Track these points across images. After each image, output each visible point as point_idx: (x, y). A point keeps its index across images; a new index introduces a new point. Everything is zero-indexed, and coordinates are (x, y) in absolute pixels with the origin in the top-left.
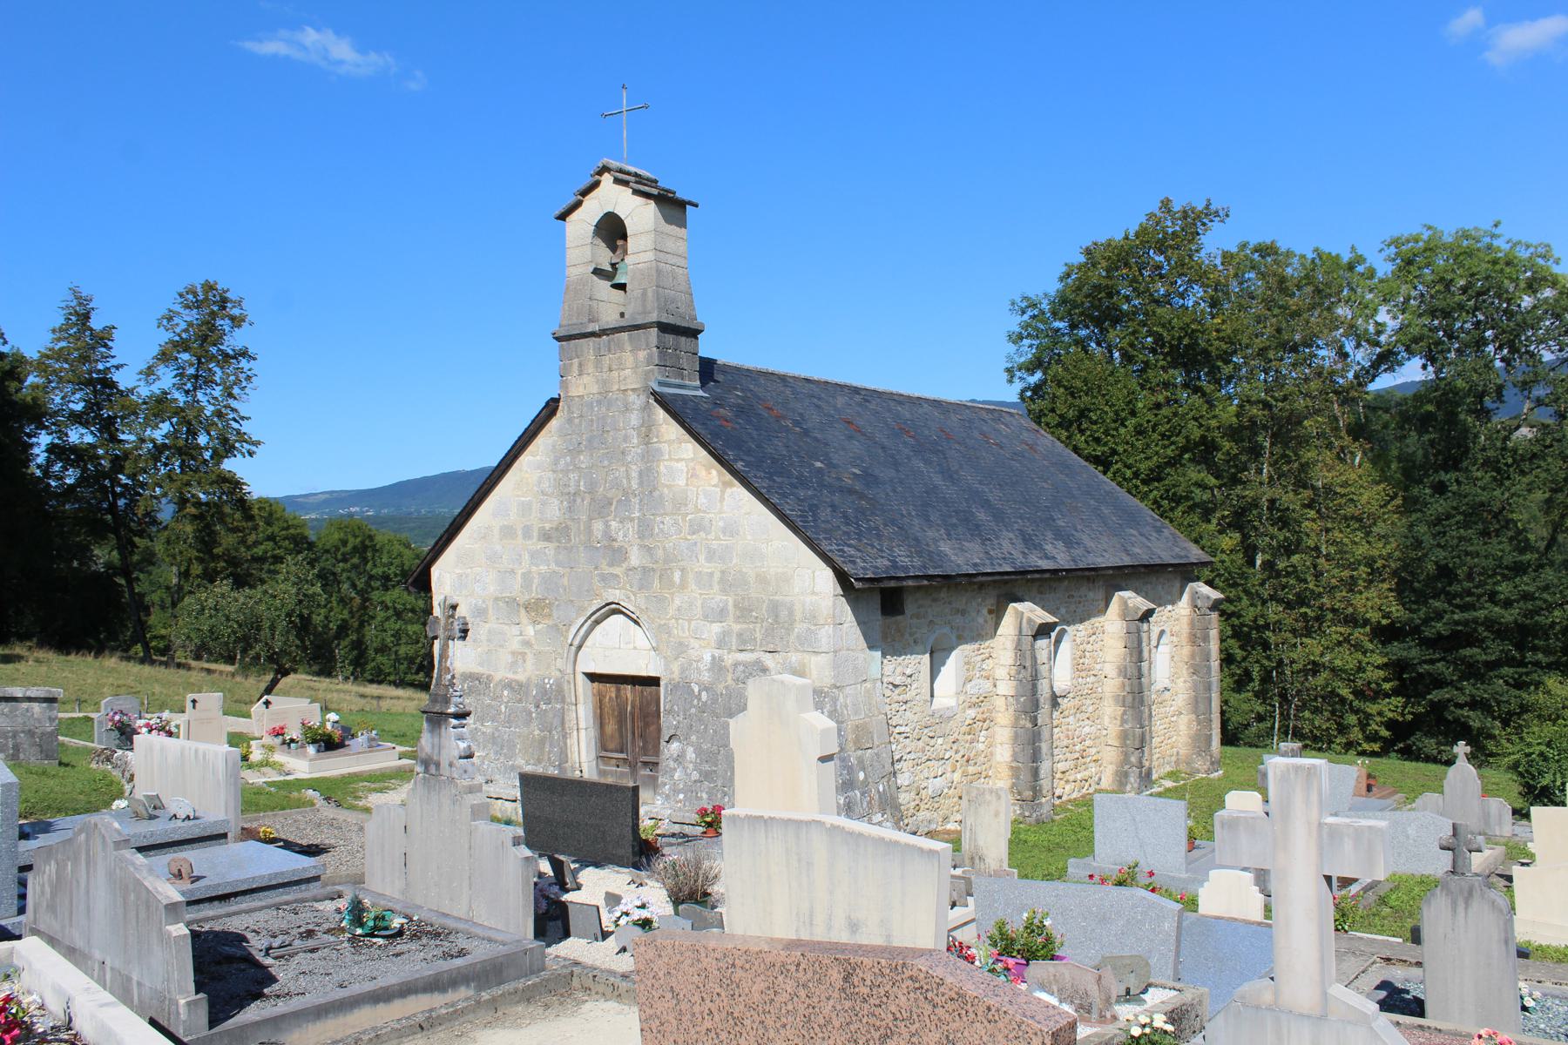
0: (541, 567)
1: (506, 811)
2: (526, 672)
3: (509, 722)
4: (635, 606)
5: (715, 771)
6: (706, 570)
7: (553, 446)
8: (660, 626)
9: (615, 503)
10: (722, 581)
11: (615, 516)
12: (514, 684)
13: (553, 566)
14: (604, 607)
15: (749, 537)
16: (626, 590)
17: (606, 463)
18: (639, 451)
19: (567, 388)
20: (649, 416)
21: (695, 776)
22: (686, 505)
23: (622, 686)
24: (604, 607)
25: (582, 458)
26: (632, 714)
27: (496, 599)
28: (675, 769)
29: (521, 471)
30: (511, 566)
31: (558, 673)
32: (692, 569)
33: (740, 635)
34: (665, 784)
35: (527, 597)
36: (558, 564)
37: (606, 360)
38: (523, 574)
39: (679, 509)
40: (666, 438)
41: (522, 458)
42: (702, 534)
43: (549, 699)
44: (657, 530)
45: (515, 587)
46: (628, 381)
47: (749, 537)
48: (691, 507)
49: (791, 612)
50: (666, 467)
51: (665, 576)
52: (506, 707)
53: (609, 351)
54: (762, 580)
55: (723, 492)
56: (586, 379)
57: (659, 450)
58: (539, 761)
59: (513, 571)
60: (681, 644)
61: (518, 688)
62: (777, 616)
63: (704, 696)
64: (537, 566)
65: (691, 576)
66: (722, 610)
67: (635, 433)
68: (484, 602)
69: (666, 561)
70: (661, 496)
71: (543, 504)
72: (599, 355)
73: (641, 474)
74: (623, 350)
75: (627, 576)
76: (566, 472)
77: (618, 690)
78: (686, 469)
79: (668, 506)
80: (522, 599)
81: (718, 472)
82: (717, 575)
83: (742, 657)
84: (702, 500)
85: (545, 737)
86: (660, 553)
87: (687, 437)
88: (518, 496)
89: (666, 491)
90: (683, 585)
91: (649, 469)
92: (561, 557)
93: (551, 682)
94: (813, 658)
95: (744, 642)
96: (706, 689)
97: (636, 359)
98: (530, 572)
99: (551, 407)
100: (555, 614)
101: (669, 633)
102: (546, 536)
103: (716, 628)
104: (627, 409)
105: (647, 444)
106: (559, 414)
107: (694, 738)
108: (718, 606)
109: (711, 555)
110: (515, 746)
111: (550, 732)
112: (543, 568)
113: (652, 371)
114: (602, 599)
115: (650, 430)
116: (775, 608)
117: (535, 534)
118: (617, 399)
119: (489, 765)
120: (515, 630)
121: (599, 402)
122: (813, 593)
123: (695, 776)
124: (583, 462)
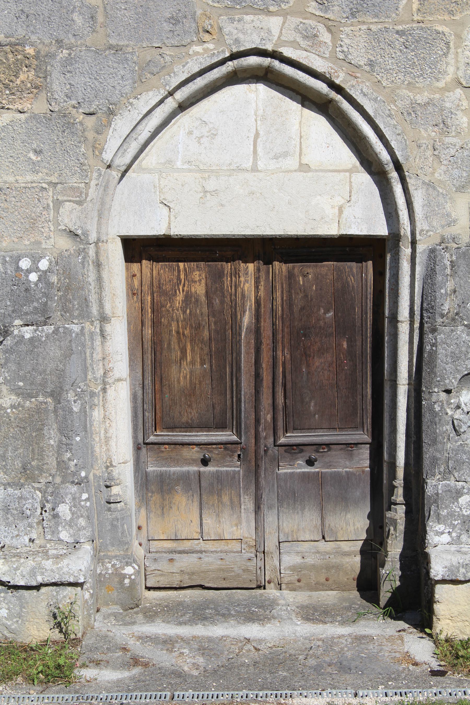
4: (333, 58)
8: (414, 106)
14: (222, 62)
16: (305, 14)
23: (228, 267)
24: (222, 62)
34: (459, 493)
93: (44, 265)
114: (220, 41)
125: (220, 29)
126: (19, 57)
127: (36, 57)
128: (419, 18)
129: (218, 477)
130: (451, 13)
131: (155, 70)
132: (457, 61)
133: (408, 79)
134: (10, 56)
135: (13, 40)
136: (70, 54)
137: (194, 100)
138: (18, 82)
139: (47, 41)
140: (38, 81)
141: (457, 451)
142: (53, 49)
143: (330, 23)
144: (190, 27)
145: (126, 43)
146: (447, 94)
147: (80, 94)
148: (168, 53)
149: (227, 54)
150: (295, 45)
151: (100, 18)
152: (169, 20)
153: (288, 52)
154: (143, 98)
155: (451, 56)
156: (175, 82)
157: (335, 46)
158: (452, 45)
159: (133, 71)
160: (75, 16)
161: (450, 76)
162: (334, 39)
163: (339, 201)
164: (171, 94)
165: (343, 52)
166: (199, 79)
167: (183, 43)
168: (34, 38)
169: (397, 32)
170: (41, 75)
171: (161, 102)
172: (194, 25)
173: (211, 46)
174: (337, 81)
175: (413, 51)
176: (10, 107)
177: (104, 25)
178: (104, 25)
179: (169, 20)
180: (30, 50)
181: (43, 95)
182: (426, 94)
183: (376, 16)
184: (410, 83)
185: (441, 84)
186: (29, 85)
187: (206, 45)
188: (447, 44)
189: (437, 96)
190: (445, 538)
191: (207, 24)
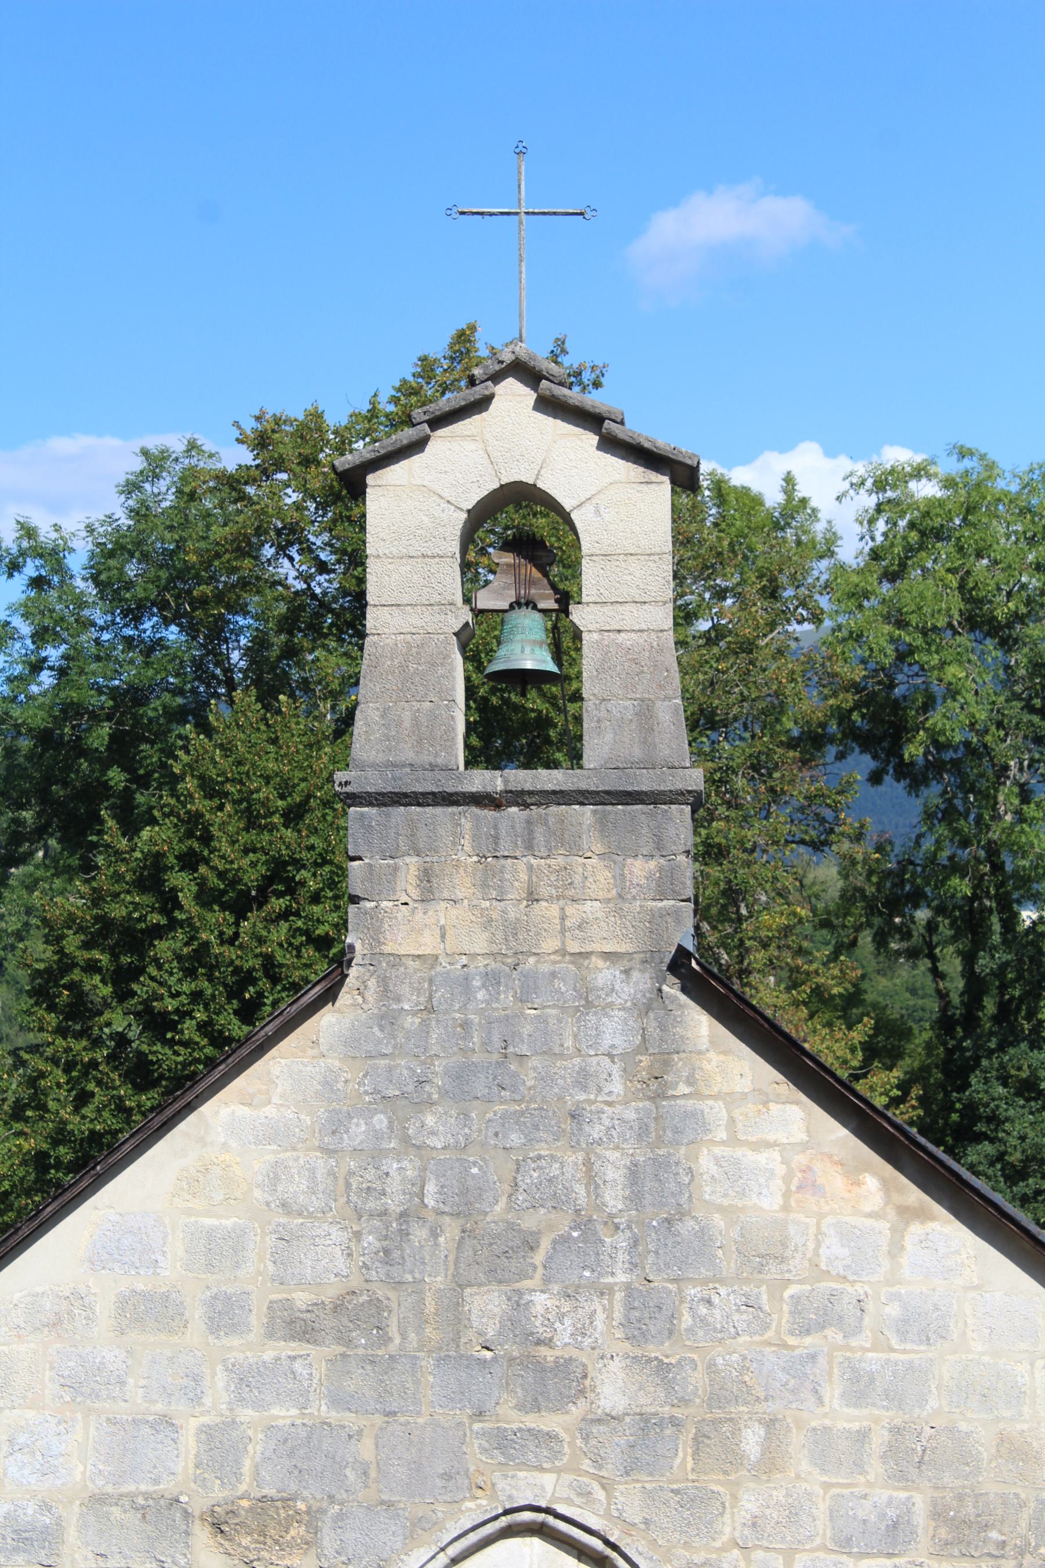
0: (276, 1411)
4: (608, 1515)
7: (326, 1083)
9: (545, 1244)
10: (891, 1452)
11: (547, 1280)
13: (321, 1409)
14: (496, 1518)
18: (630, 1115)
19: (379, 931)
20: (663, 1027)
22: (782, 1260)
24: (496, 1518)
27: (99, 1500)
29: (202, 1141)
30: (159, 1407)
35: (218, 1493)
36: (337, 1401)
38: (207, 1432)
39: (760, 1269)
41: (207, 1109)
42: (833, 1335)
44: (687, 1320)
48: (797, 1265)
50: (717, 1162)
56: (441, 913)
57: (692, 1115)
59: (166, 1423)
64: (259, 1405)
65: (796, 1439)
66: (895, 1525)
67: (616, 1069)
68: (45, 1507)
69: (714, 1400)
70: (703, 1234)
73: (634, 1173)
74: (574, 848)
75: (586, 1438)
76: (376, 1155)
78: (781, 1170)
79: (728, 1264)
80: (198, 1505)
81: (886, 1185)
82: (879, 1439)
86: (697, 1380)
87: (785, 1088)
88: (189, 1212)
89: (718, 1221)
91: (661, 1165)
97: (621, 878)
100: (328, 1540)
104: (589, 1004)
106: (345, 997)
108: (882, 1516)
112: (284, 1414)
113: (676, 914)
114: (493, 1497)
115: (666, 1064)
117: (256, 1320)
118: (553, 975)
121: (491, 979)
124: (433, 1133)
125: (493, 1485)
126: (290, 1513)
127: (308, 1512)
128: (694, 1477)
130: (726, 1473)
131: (427, 1526)
132: (733, 1521)
133: (684, 1538)
134: (282, 1511)
135: (285, 1495)
136: (341, 1510)
137: (466, 1554)
138: (288, 1538)
139: (318, 1497)
140: (309, 1537)
142: (325, 1505)
143: (604, 1481)
144: (462, 1483)
145: (398, 1498)
146: (724, 1554)
147: (350, 1550)
148: (440, 1509)
149: (500, 1511)
150: (569, 1501)
151: (373, 1474)
152: (441, 1476)
153: (561, 1509)
154: (415, 1553)
155: (727, 1516)
157: (609, 1504)
158: (727, 1504)
159: (405, 1527)
160: (348, 1472)
161: (727, 1536)
162: (609, 1497)
164: (442, 1549)
165: (618, 1509)
166: (471, 1534)
167: (456, 1499)
168: (306, 1493)
169: (672, 1491)
170: (311, 1531)
171: (433, 1557)
172: (466, 1481)
173: (484, 1502)
174: (612, 1539)
175: (688, 1510)
176: (279, 1562)
177: (377, 1481)
178: (377, 1481)
179: (441, 1476)
180: (301, 1506)
181: (313, 1551)
182: (702, 1553)
183: (651, 1474)
184: (686, 1543)
185: (718, 1544)
186: (299, 1541)
187: (479, 1501)
188: (723, 1503)
189: (714, 1556)
191: (480, 1480)
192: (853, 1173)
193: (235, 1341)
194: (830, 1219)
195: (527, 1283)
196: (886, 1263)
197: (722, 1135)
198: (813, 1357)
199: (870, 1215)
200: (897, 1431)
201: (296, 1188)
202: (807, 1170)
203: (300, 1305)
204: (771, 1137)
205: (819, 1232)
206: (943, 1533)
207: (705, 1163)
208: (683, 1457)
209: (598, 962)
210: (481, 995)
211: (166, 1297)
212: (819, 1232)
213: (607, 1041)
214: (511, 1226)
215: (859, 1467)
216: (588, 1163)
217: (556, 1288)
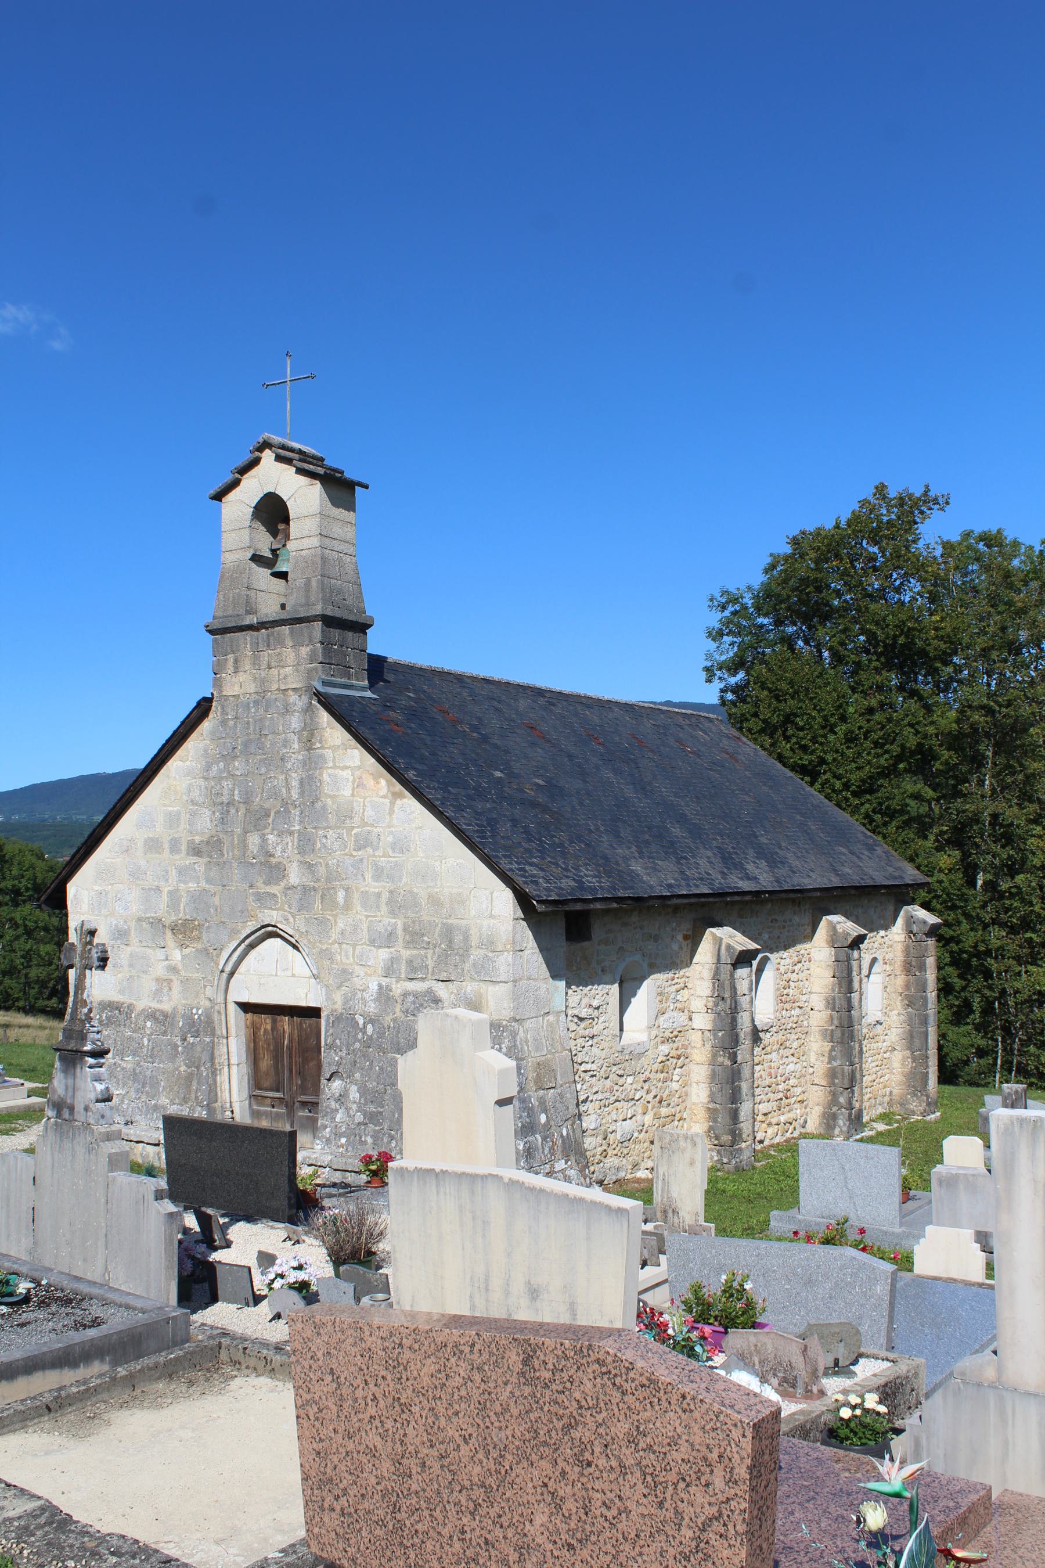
0: (190, 885)
1: (148, 1156)
2: (172, 1001)
3: (152, 1057)
4: (294, 929)
5: (381, 1113)
6: (372, 890)
7: (205, 751)
8: (322, 951)
9: (272, 814)
10: (390, 902)
11: (273, 829)
12: (158, 1014)
13: (203, 884)
15: (421, 854)
17: (263, 770)
18: (301, 757)
19: (221, 686)
20: (311, 719)
21: (359, 1117)
22: (351, 818)
25: (237, 764)
26: (290, 1048)
28: (337, 1111)
29: (168, 777)
31: (208, 1004)
32: (357, 889)
33: (410, 962)
34: (326, 1127)
35: (174, 918)
36: (209, 881)
37: (265, 657)
38: (170, 892)
40: (330, 742)
41: (169, 763)
42: (369, 850)
43: (198, 1031)
44: (319, 845)
45: (161, 907)
46: (289, 679)
47: (421, 854)
48: (357, 820)
49: (467, 938)
51: (327, 895)
52: (149, 1040)
53: (268, 646)
54: (435, 901)
55: (392, 804)
56: (242, 677)
57: (321, 756)
58: (185, 1100)
59: (158, 889)
60: (344, 971)
61: (162, 1019)
62: (450, 942)
63: (370, 1029)
64: (185, 883)
65: (356, 896)
67: (296, 738)
68: (125, 922)
69: (329, 880)
70: (324, 807)
71: (193, 814)
72: (256, 651)
76: (219, 779)
77: (274, 1022)
78: (351, 778)
79: (332, 819)
80: (168, 920)
81: (387, 781)
82: (385, 896)
83: (412, 986)
84: (370, 813)
85: (192, 1074)
86: (322, 870)
87: (353, 742)
88: (165, 805)
89: (329, 802)
90: (347, 907)
91: (311, 778)
92: (212, 874)
93: (200, 1012)
94: (490, 988)
95: (415, 970)
96: (372, 1021)
97: (298, 656)
98: (178, 890)
99: (203, 708)
100: (205, 937)
101: (331, 959)
102: (196, 851)
103: (384, 954)
105: (310, 749)
106: (211, 715)
107: (357, 1076)
109: (378, 875)
110: (158, 1083)
111: (198, 1068)
112: (192, 886)
113: (315, 669)
114: (257, 921)
115: (312, 735)
116: (448, 933)
117: (184, 848)
119: (128, 1104)
120: (160, 954)
121: (256, 703)
122: (491, 916)
123: (359, 1117)
129: (277, 1114)
141: (327, 1107)
150: (281, 922)
153: (279, 926)
156: (242, 937)
163: (306, 991)
190: (319, 1147)
192: (376, 778)
193: (177, 857)
194: (368, 799)
195: (267, 831)
196: (387, 817)
197: (331, 764)
198: (361, 860)
199: (382, 797)
200: (391, 892)
201: (196, 794)
202: (360, 778)
203: (197, 842)
204: (348, 764)
205: (364, 805)
206: (407, 937)
207: (325, 777)
208: (318, 905)
209: (291, 693)
210: (253, 710)
211: (157, 839)
212: (364, 805)
213: (293, 726)
214: (262, 807)
215: (378, 908)
216: (286, 779)
217: (275, 832)
